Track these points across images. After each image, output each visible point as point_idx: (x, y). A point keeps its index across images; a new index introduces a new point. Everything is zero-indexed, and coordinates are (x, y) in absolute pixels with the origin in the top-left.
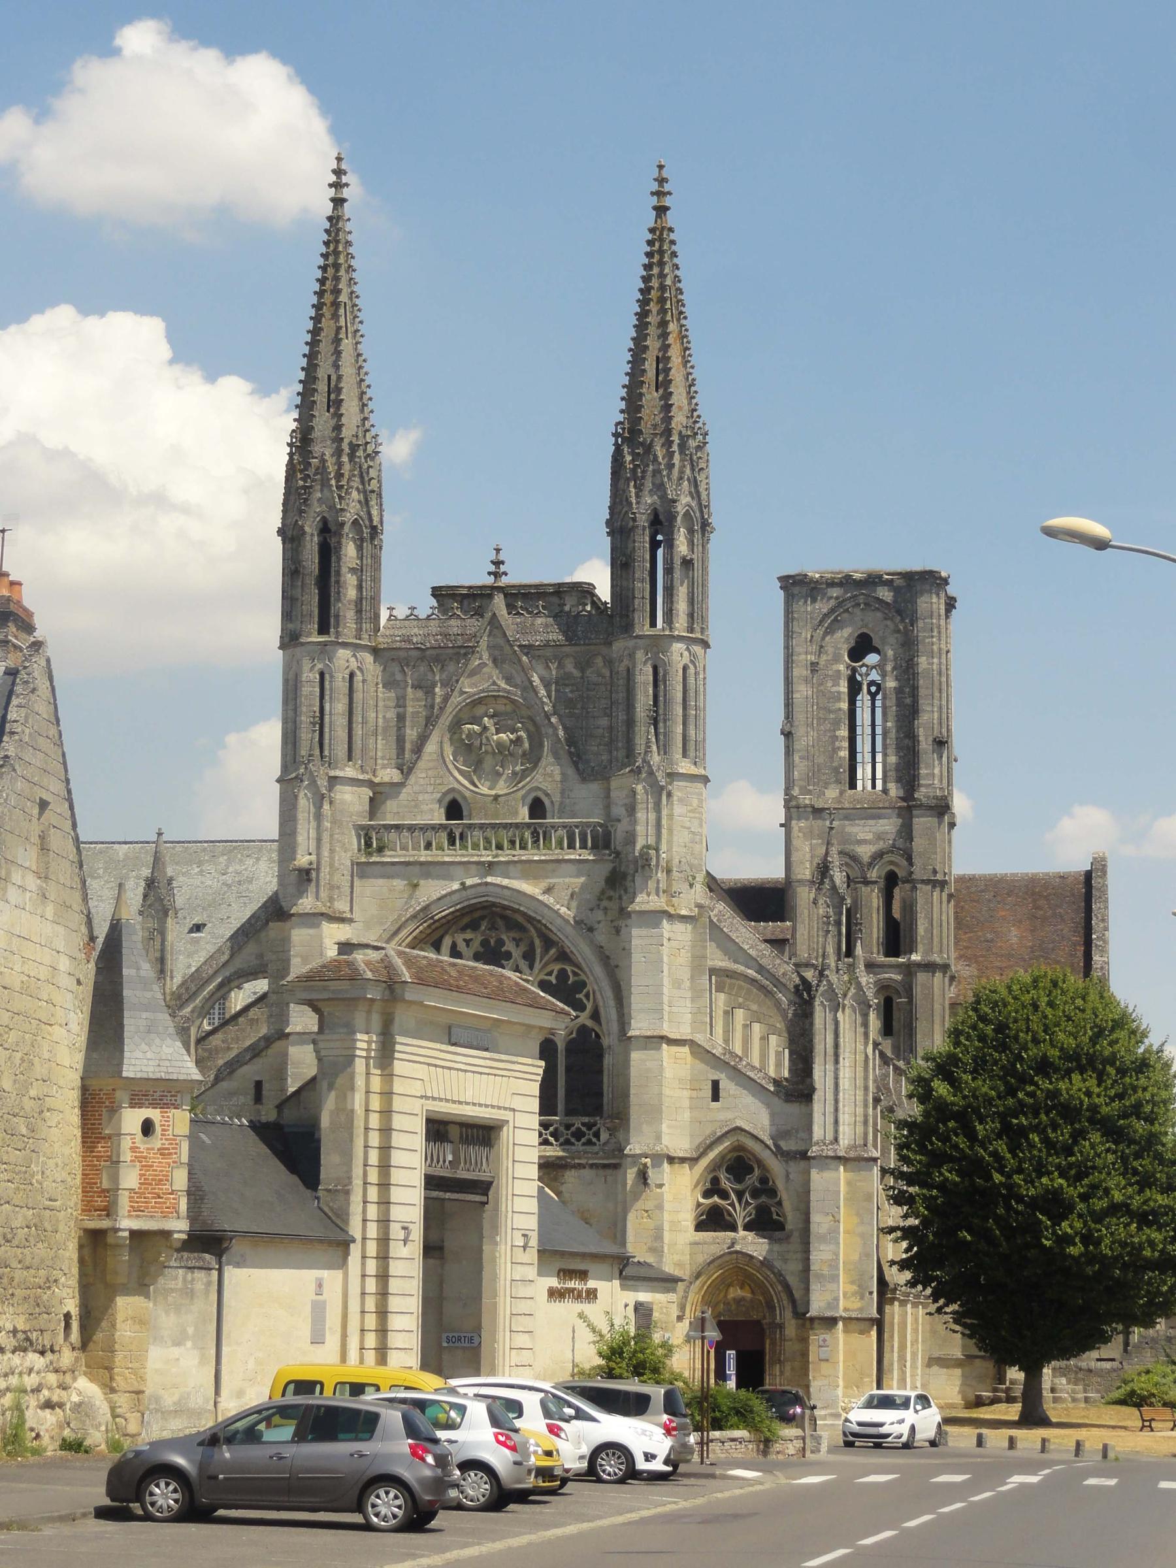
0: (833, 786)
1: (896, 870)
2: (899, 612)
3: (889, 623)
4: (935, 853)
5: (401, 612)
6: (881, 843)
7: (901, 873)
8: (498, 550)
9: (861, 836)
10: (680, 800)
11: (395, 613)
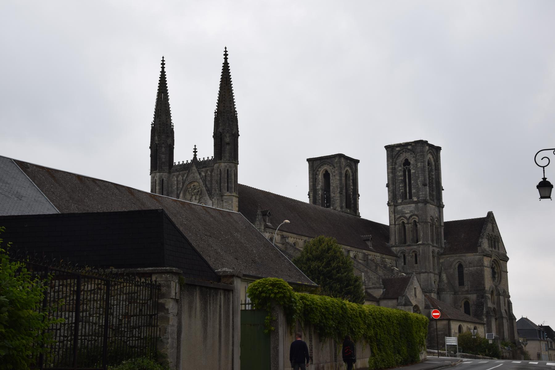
0: (400, 199)
1: (416, 220)
2: (413, 152)
3: (412, 155)
5: (177, 164)
6: (412, 213)
7: (417, 221)
8: (195, 146)
9: (406, 212)
10: (225, 202)
11: (176, 164)
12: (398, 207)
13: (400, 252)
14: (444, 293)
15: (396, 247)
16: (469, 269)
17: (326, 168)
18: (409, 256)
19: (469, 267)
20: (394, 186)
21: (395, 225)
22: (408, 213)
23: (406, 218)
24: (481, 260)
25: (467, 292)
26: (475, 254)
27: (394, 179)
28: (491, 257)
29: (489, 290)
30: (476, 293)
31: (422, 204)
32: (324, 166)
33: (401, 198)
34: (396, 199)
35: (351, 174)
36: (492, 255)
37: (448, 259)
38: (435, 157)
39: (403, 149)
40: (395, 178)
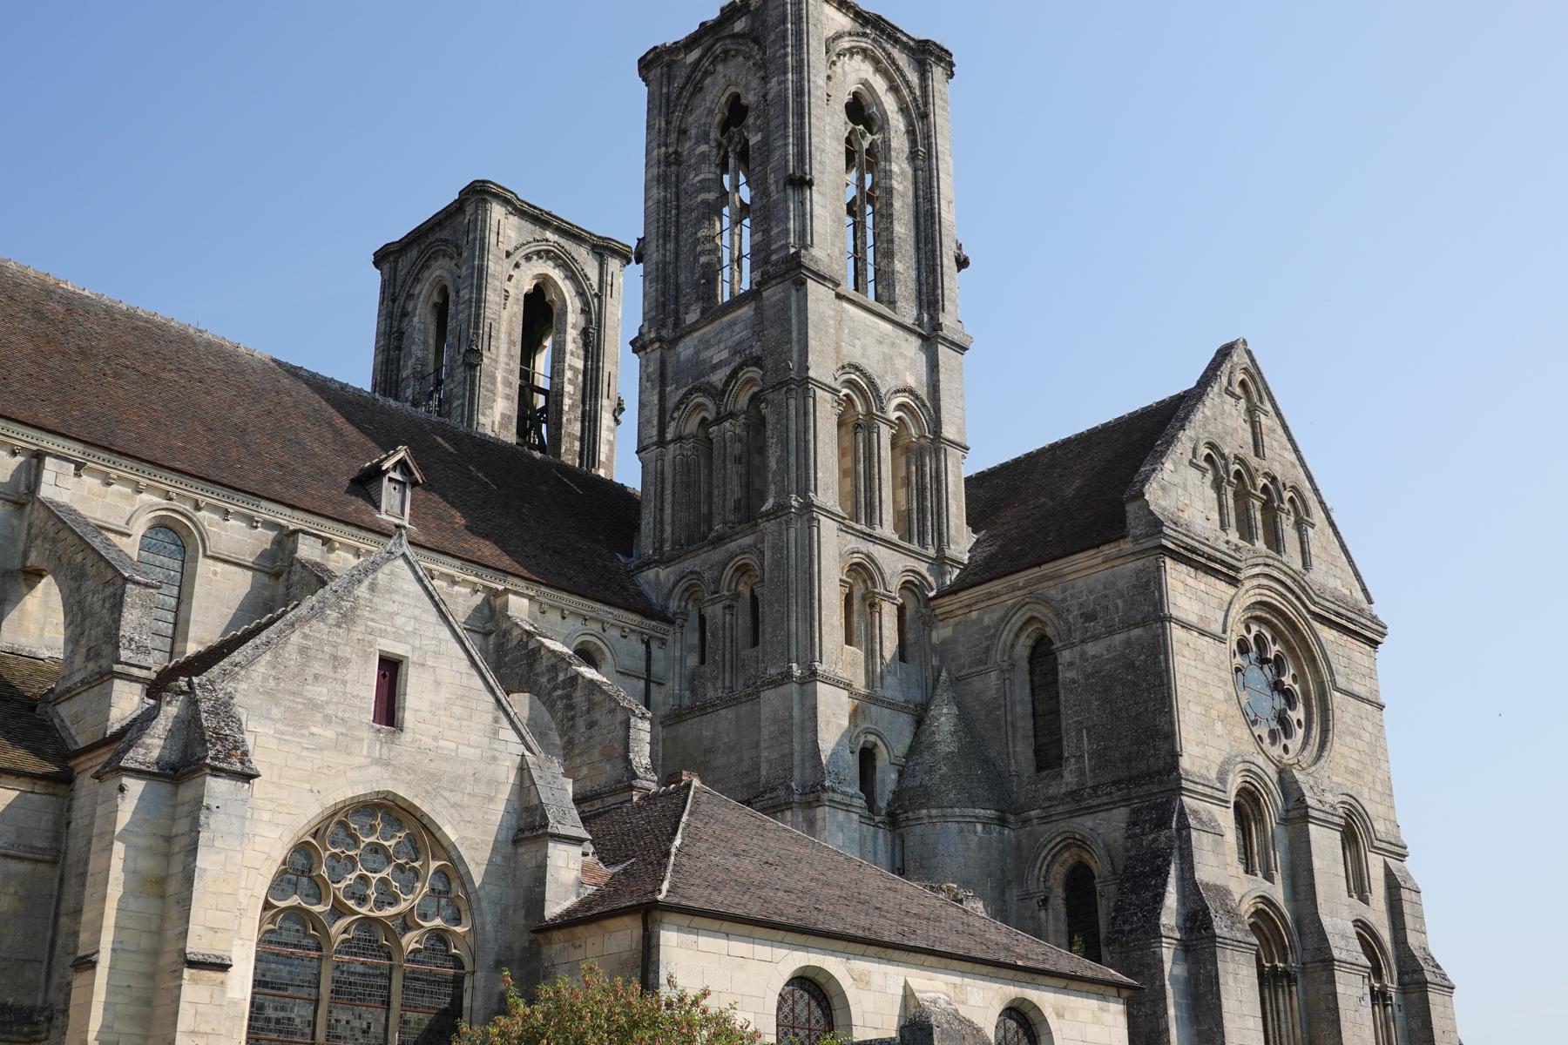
2: (756, 41)
4: (789, 341)
12: (681, 347)
13: (678, 590)
14: (924, 812)
15: (658, 563)
16: (1083, 653)
17: (438, 273)
18: (713, 602)
19: (1083, 641)
20: (671, 246)
21: (662, 442)
22: (721, 364)
23: (709, 390)
24: (1147, 583)
25: (1078, 802)
26: (1108, 550)
27: (673, 212)
28: (1234, 581)
29: (1213, 775)
30: (1126, 800)
31: (780, 287)
32: (435, 265)
33: (697, 300)
34: (677, 312)
35: (573, 305)
36: (1238, 570)
37: (974, 615)
38: (905, 92)
39: (709, 49)
40: (678, 207)
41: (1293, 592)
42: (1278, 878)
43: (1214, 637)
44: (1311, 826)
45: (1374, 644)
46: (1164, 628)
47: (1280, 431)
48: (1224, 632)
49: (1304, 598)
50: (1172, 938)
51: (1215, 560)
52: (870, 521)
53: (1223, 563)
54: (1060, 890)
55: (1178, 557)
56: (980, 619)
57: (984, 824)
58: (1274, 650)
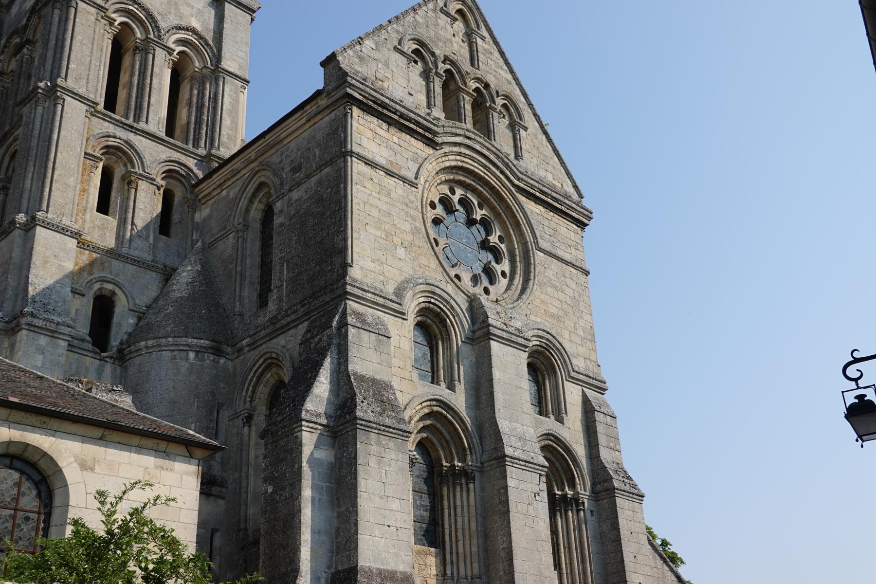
14: (143, 343)
28: (432, 143)
29: (390, 289)
36: (435, 134)
41: (498, 167)
42: (460, 387)
43: (404, 180)
44: (492, 342)
45: (582, 225)
46: (346, 162)
47: (497, 54)
48: (416, 178)
49: (508, 173)
50: (316, 423)
51: (410, 120)
52: (137, 119)
53: (417, 123)
54: (264, 408)
55: (366, 109)
56: (228, 195)
57: (197, 352)
58: (478, 214)
